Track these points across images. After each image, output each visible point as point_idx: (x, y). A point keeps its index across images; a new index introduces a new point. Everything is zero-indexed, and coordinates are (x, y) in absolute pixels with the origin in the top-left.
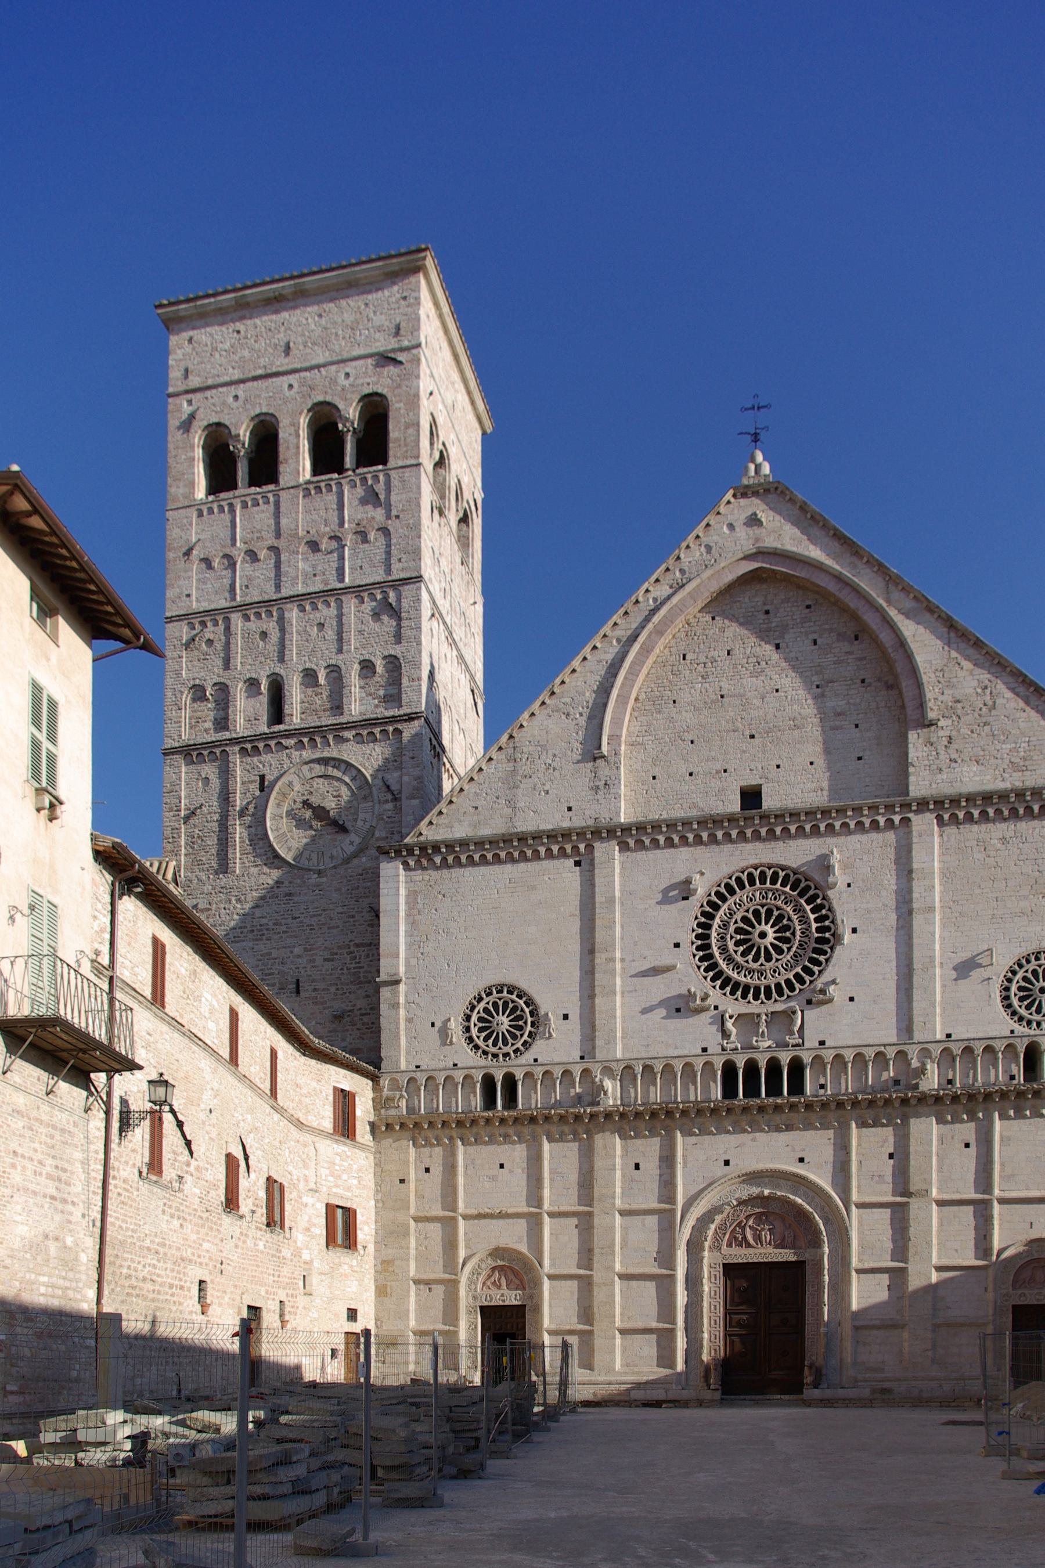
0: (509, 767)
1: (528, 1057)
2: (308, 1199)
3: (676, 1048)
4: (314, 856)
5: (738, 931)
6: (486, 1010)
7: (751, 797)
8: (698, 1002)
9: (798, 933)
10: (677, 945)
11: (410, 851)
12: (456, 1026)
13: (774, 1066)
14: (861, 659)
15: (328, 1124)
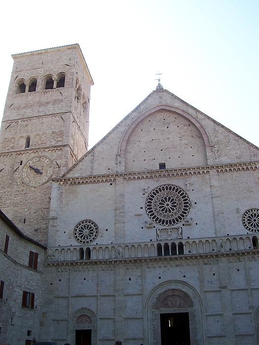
0: (92, 158)
1: (94, 243)
2: (17, 290)
3: (142, 240)
4: (34, 183)
5: (160, 204)
6: (82, 228)
7: (162, 166)
8: (148, 225)
9: (178, 204)
10: (141, 208)
11: (61, 181)
12: (72, 232)
13: (174, 245)
14: (191, 131)
15: (27, 264)
